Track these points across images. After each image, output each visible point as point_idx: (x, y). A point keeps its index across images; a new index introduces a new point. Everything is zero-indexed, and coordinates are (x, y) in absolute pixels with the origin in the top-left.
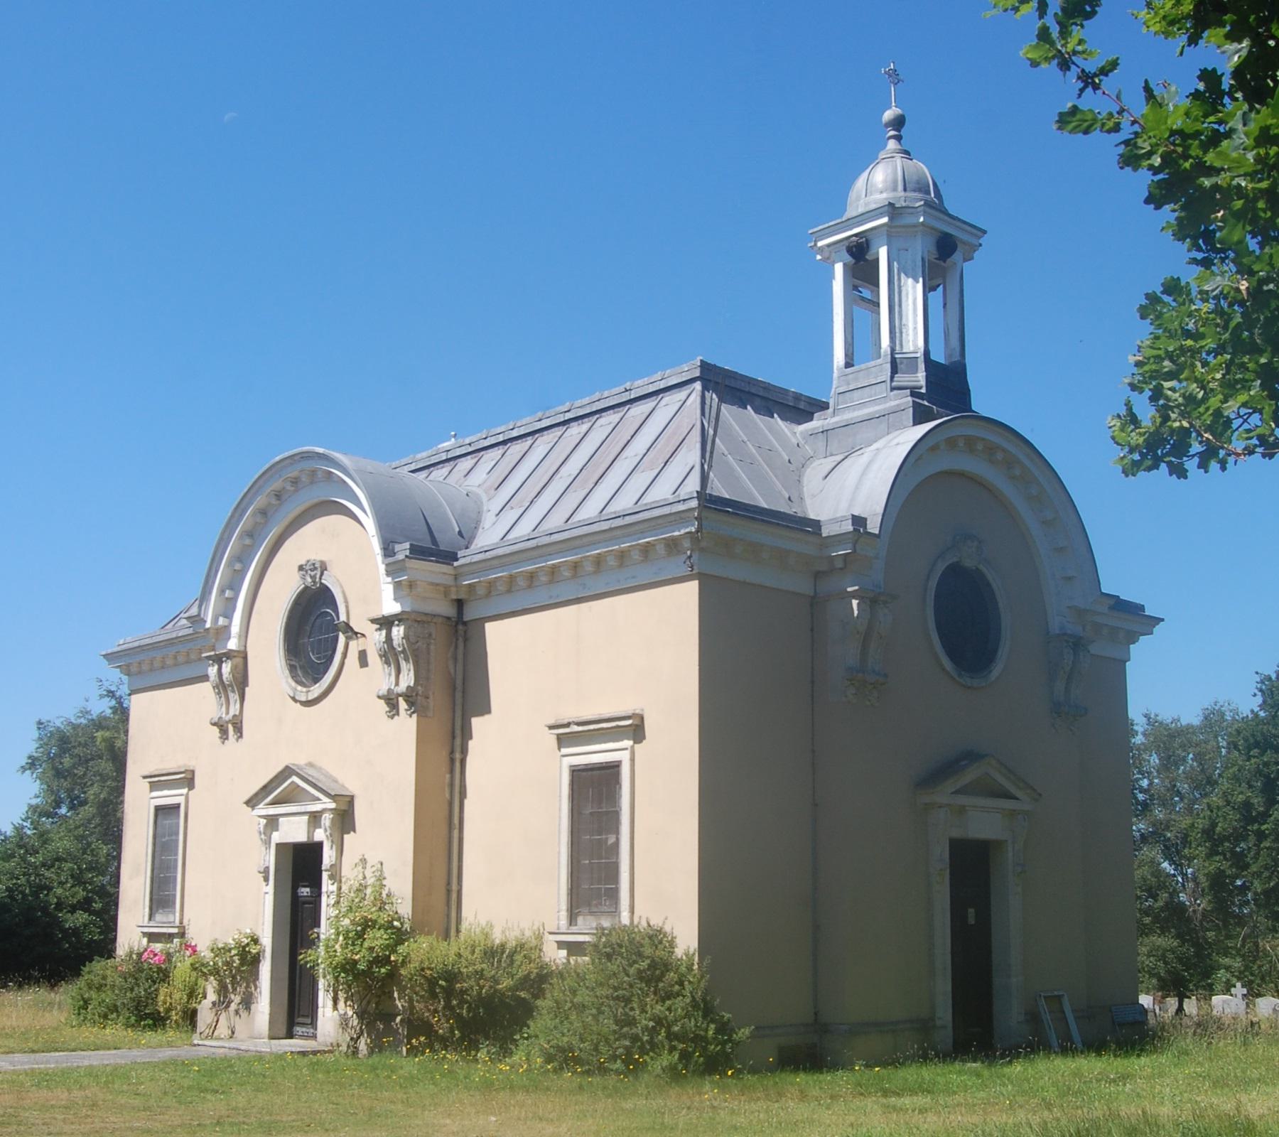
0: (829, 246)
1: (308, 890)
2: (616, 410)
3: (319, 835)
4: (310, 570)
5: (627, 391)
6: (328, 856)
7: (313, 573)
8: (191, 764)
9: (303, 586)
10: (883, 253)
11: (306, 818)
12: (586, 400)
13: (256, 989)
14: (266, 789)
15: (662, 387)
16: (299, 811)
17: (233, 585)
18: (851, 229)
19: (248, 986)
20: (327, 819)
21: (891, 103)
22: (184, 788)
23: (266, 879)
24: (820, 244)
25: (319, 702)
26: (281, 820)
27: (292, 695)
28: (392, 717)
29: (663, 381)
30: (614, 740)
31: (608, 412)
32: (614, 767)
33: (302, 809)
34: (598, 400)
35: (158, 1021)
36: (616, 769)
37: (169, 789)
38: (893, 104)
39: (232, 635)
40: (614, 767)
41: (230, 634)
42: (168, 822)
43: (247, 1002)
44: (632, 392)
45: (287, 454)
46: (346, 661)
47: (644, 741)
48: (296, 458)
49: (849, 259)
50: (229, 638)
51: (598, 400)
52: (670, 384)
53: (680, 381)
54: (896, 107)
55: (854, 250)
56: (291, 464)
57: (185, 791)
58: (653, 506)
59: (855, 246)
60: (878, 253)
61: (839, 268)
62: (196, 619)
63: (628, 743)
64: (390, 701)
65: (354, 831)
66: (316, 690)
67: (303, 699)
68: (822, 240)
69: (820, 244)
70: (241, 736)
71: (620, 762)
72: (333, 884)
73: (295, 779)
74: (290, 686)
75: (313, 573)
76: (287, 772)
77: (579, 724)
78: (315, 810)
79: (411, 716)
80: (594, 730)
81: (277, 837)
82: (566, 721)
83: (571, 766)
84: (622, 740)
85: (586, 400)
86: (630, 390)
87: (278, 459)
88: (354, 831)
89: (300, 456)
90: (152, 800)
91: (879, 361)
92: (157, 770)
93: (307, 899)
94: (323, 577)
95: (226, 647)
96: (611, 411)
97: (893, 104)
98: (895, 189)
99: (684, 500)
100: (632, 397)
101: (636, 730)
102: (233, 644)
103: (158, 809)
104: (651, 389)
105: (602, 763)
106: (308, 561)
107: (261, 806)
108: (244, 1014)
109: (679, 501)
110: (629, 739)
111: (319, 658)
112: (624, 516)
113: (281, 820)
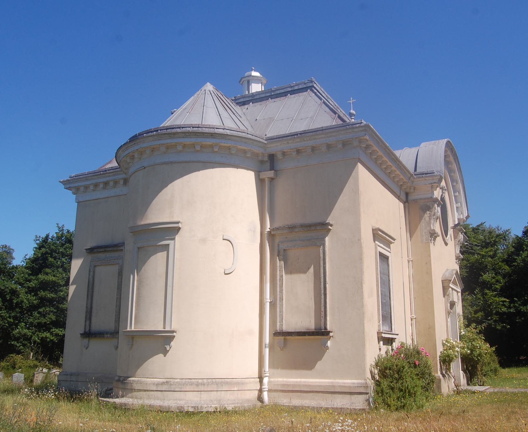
21: (351, 109)
38: (352, 109)
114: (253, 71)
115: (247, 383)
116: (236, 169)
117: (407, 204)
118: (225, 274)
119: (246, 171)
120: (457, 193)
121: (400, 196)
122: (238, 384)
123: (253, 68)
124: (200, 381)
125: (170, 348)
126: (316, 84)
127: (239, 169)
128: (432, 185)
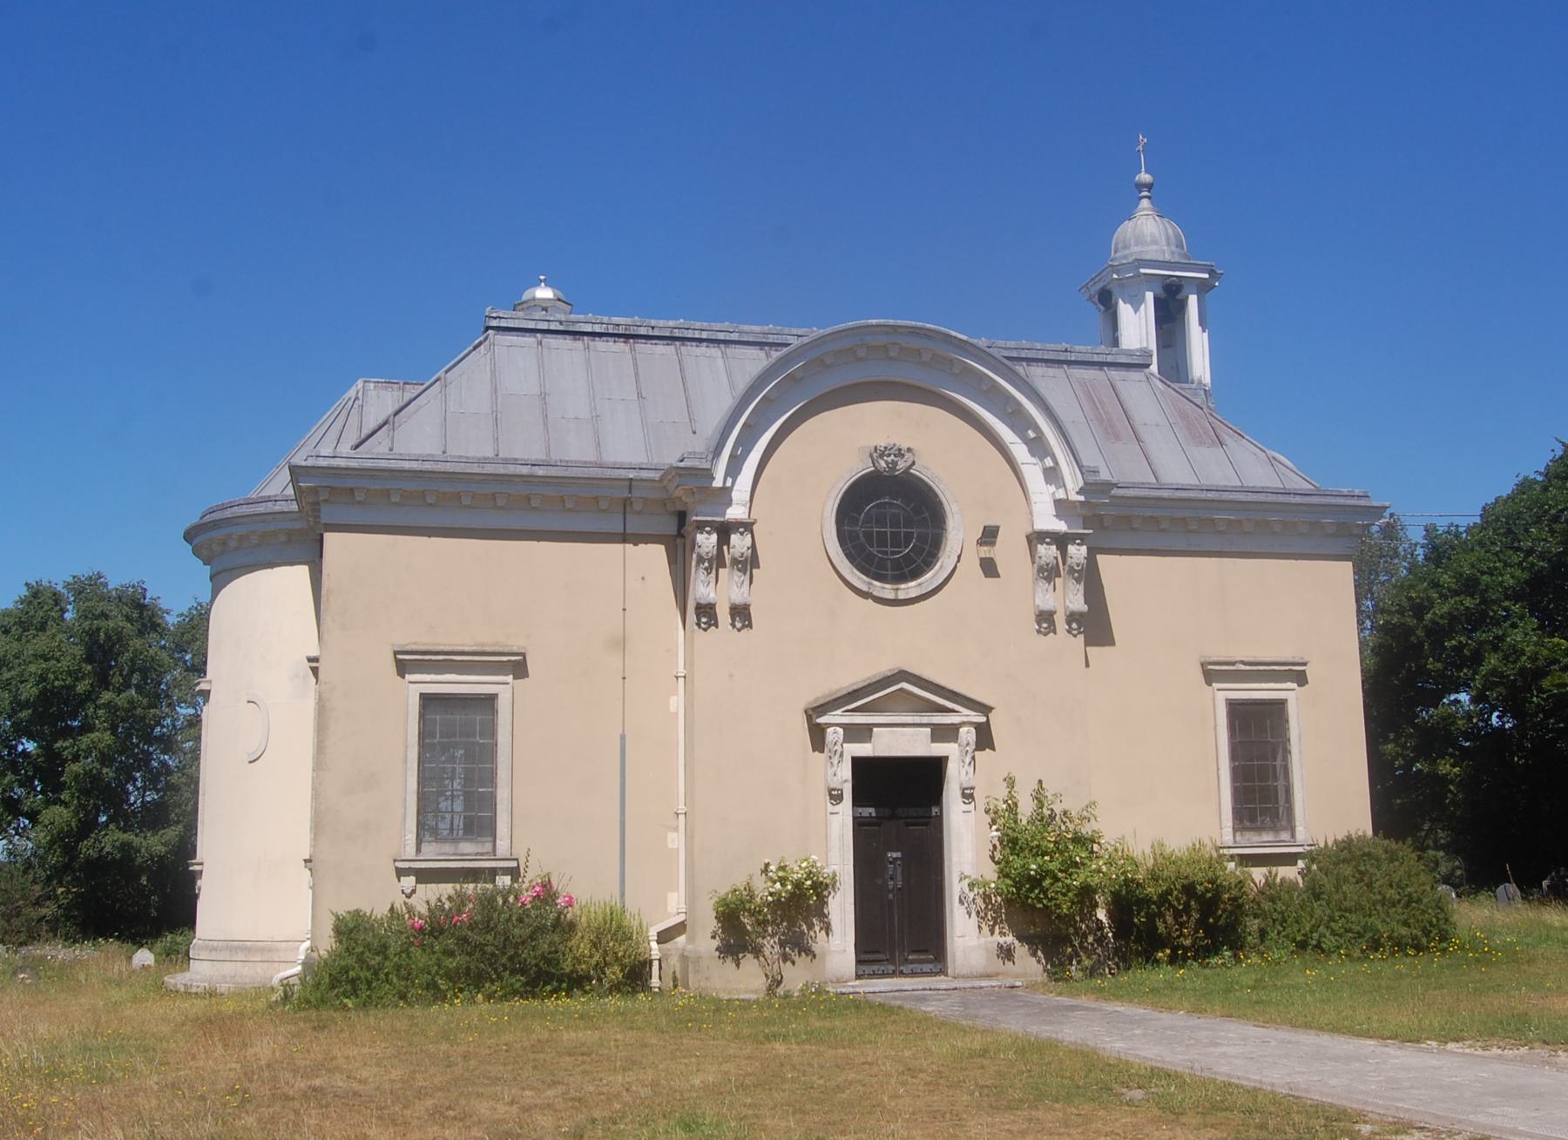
0: (1145, 274)
1: (872, 810)
2: (1049, 365)
3: (938, 749)
4: (895, 455)
5: (1066, 351)
6: (956, 776)
7: (896, 459)
8: (515, 644)
9: (873, 469)
10: (1193, 300)
11: (928, 730)
12: (1012, 344)
13: (811, 926)
14: (854, 695)
15: (1108, 360)
16: (919, 722)
17: (746, 442)
18: (1174, 271)
19: (792, 924)
20: (968, 735)
22: (507, 675)
23: (836, 797)
24: (1142, 271)
25: (913, 604)
26: (875, 729)
27: (865, 588)
28: (1045, 635)
29: (1110, 356)
30: (1276, 682)
31: (1040, 364)
32: (1281, 705)
33: (925, 720)
34: (1028, 349)
35: (576, 982)
36: (1281, 706)
37: (436, 674)
38: (1143, 169)
39: (734, 502)
40: (1281, 705)
41: (731, 500)
42: (438, 717)
43: (798, 945)
44: (1073, 354)
45: (891, 322)
46: (958, 565)
47: (1307, 686)
48: (900, 330)
49: (1160, 291)
50: (729, 503)
51: (1028, 349)
52: (1118, 361)
53: (1131, 362)
54: (1146, 172)
55: (1174, 288)
56: (887, 333)
57: (510, 678)
58: (1327, 493)
59: (1176, 286)
60: (1187, 298)
61: (1150, 296)
62: (706, 473)
63: (1294, 685)
64: (1045, 619)
65: (994, 749)
66: (910, 589)
67: (890, 595)
68: (1144, 268)
69: (1142, 271)
70: (750, 626)
71: (1286, 700)
72: (970, 803)
73: (905, 685)
74: (859, 578)
75: (896, 459)
76: (903, 675)
77: (1243, 663)
78: (949, 722)
79: (1075, 636)
80: (1265, 670)
81: (864, 750)
82: (1233, 660)
83: (1227, 700)
84: (1285, 682)
85: (1012, 344)
86: (1070, 352)
87: (874, 322)
88: (994, 749)
89: (912, 330)
90: (411, 685)
91: (1194, 386)
92: (415, 643)
93: (867, 820)
94: (914, 467)
95: (724, 514)
96: (1044, 364)
97: (1143, 169)
98: (1182, 248)
99: (1358, 496)
100: (1073, 359)
101: (1301, 679)
102: (735, 512)
103: (426, 699)
104: (1096, 358)
105: (1264, 700)
106: (895, 445)
107: (839, 712)
108: (802, 960)
109: (1353, 496)
110: (1292, 682)
111: (878, 552)
112: (1295, 494)
113: (875, 729)
114: (543, 284)
115: (277, 950)
116: (269, 570)
117: (678, 540)
118: (250, 762)
119: (269, 571)
120: (1030, 432)
121: (627, 531)
122: (262, 950)
123: (542, 277)
124: (215, 944)
125: (200, 889)
126: (500, 318)
127: (275, 569)
128: (683, 489)
